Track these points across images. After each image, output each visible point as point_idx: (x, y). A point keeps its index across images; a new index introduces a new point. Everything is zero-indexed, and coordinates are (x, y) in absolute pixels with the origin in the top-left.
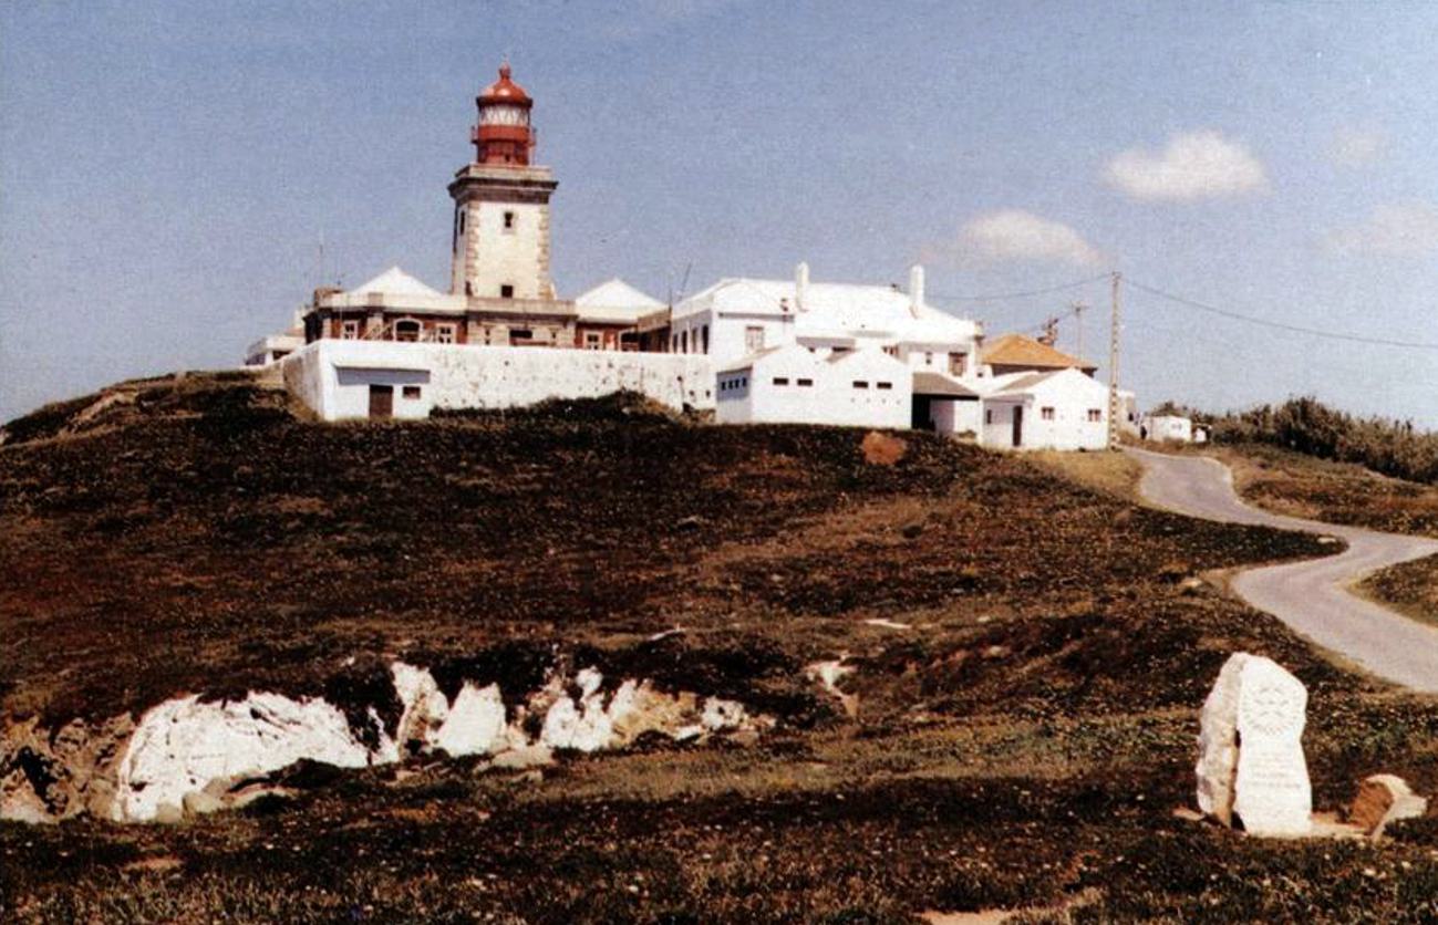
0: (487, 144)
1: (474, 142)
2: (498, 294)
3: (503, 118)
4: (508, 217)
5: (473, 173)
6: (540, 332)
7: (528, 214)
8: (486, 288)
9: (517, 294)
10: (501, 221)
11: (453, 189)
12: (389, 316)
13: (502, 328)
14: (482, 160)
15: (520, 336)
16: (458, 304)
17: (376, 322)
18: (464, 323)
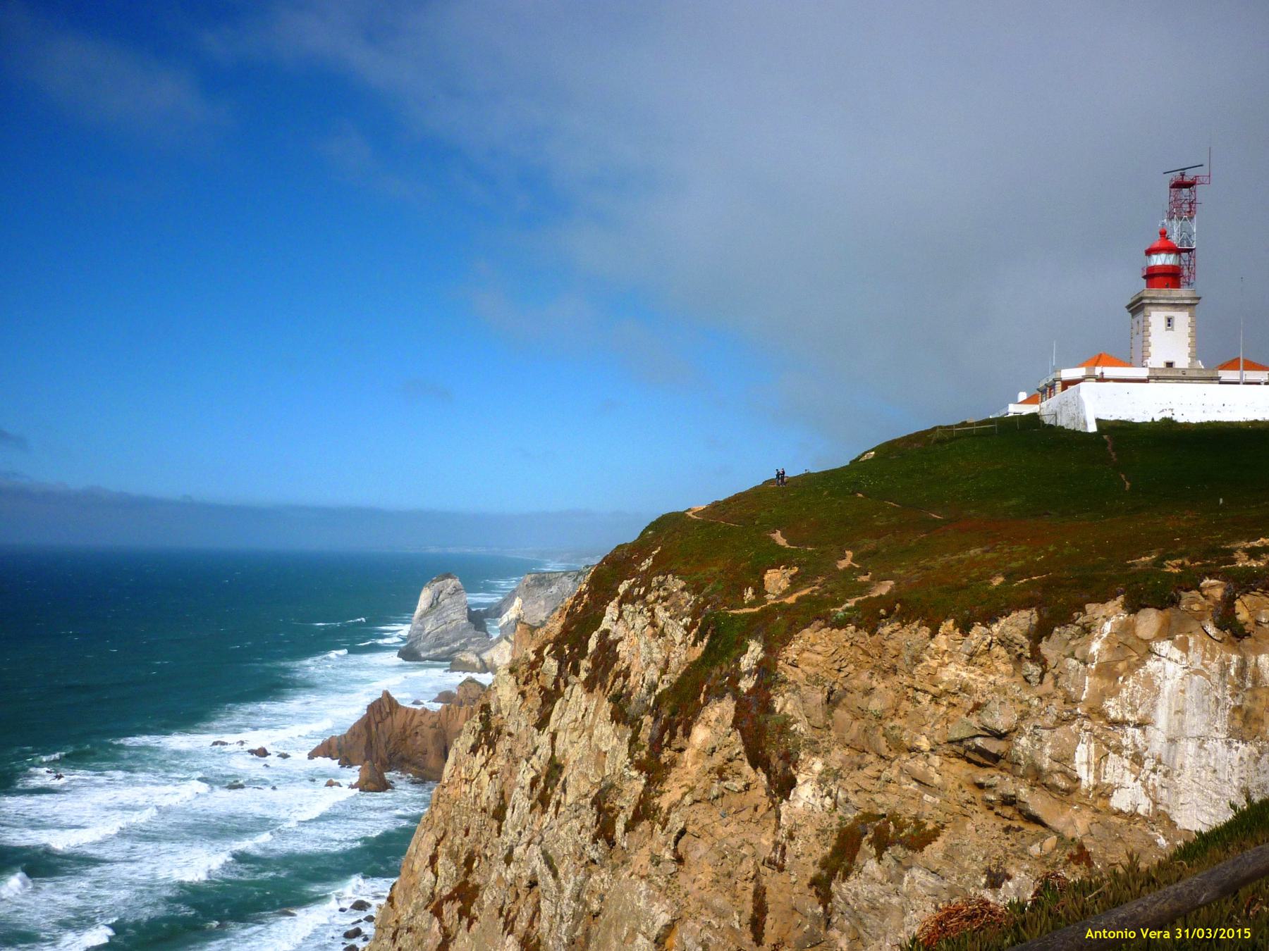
0: (1154, 276)
1: (1144, 277)
2: (1163, 366)
5: (1146, 295)
7: (1182, 319)
9: (1177, 366)
10: (1164, 323)
14: (1149, 285)
16: (1143, 373)
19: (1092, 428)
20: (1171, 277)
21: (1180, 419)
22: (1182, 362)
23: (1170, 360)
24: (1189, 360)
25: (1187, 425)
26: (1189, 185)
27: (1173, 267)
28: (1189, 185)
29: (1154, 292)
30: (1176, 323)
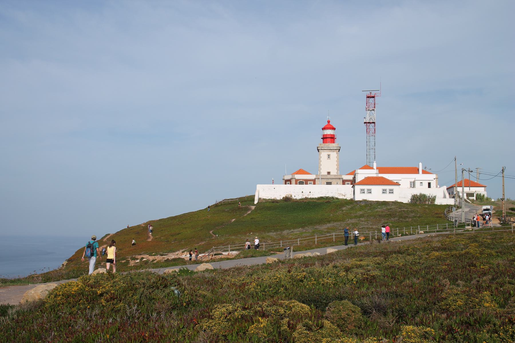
0: (325, 138)
1: (323, 138)
2: (326, 174)
3: (329, 132)
4: (329, 155)
6: (333, 181)
8: (324, 172)
9: (331, 174)
10: (327, 157)
11: (318, 150)
12: (296, 180)
13: (325, 181)
15: (329, 183)
16: (313, 177)
17: (293, 181)
18: (314, 182)
19: (256, 202)
20: (332, 138)
21: (293, 197)
22: (334, 172)
23: (329, 171)
24: (336, 171)
25: (296, 199)
26: (373, 97)
27: (331, 135)
28: (373, 97)
29: (323, 145)
30: (331, 157)
